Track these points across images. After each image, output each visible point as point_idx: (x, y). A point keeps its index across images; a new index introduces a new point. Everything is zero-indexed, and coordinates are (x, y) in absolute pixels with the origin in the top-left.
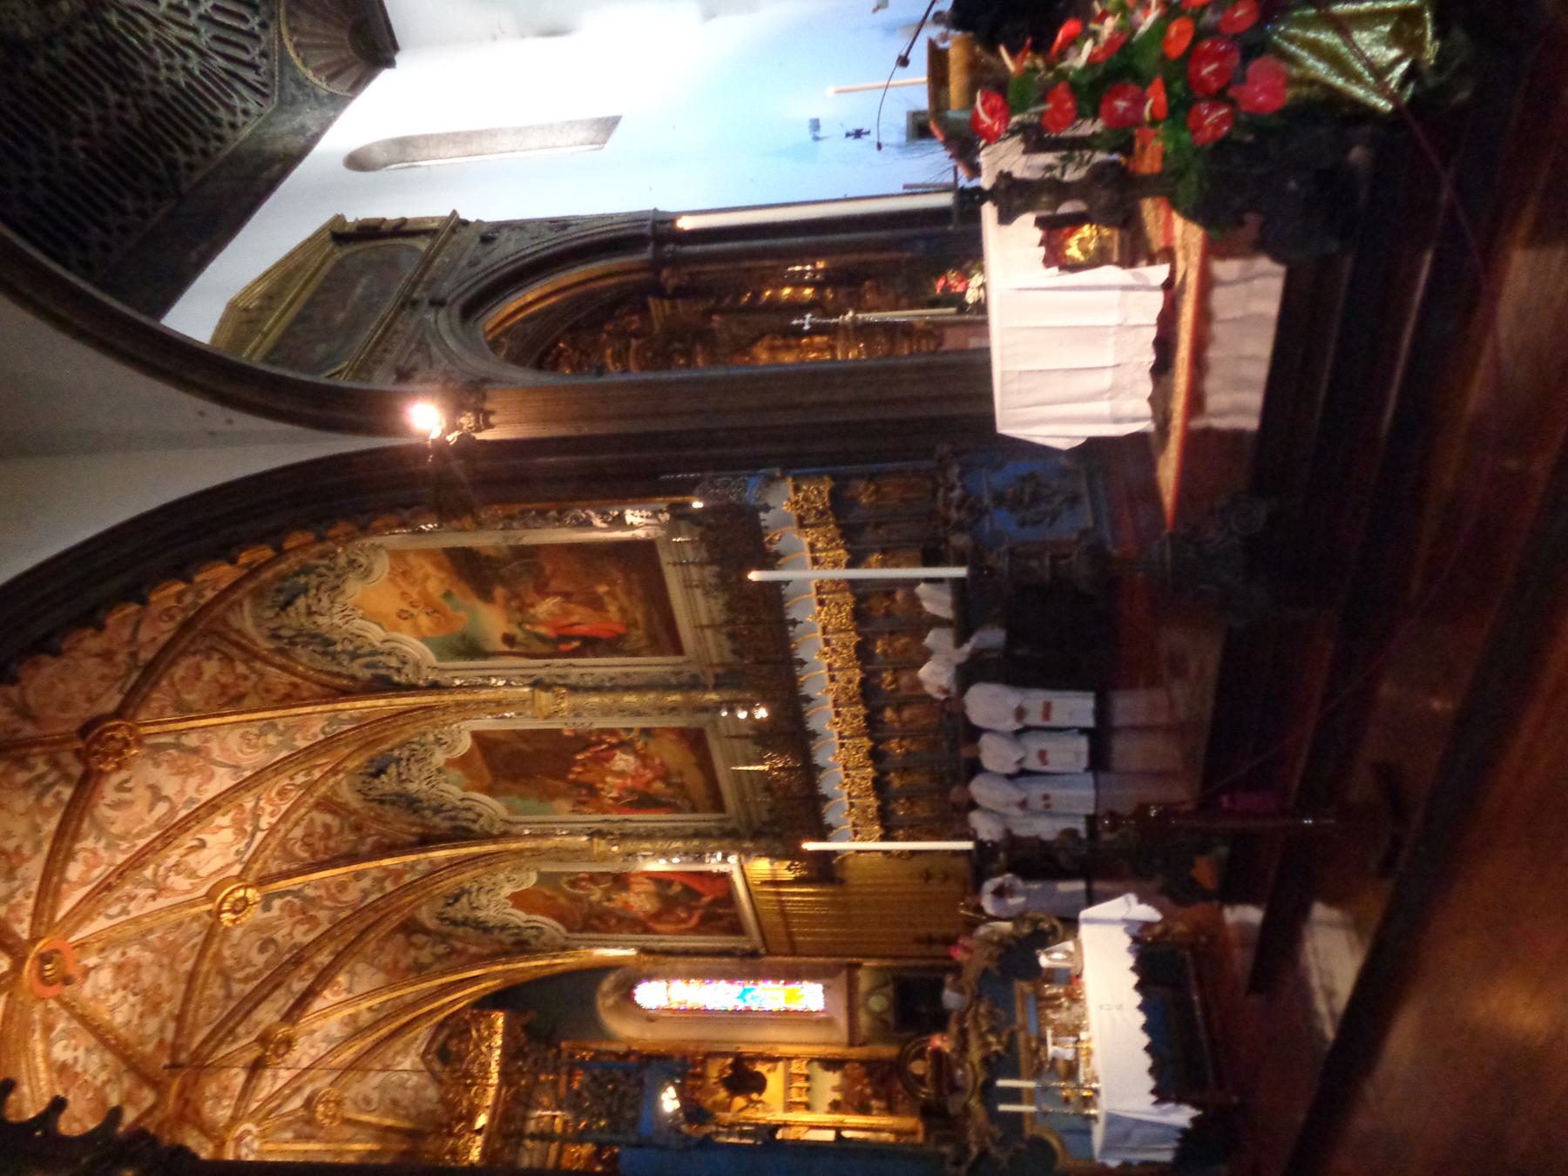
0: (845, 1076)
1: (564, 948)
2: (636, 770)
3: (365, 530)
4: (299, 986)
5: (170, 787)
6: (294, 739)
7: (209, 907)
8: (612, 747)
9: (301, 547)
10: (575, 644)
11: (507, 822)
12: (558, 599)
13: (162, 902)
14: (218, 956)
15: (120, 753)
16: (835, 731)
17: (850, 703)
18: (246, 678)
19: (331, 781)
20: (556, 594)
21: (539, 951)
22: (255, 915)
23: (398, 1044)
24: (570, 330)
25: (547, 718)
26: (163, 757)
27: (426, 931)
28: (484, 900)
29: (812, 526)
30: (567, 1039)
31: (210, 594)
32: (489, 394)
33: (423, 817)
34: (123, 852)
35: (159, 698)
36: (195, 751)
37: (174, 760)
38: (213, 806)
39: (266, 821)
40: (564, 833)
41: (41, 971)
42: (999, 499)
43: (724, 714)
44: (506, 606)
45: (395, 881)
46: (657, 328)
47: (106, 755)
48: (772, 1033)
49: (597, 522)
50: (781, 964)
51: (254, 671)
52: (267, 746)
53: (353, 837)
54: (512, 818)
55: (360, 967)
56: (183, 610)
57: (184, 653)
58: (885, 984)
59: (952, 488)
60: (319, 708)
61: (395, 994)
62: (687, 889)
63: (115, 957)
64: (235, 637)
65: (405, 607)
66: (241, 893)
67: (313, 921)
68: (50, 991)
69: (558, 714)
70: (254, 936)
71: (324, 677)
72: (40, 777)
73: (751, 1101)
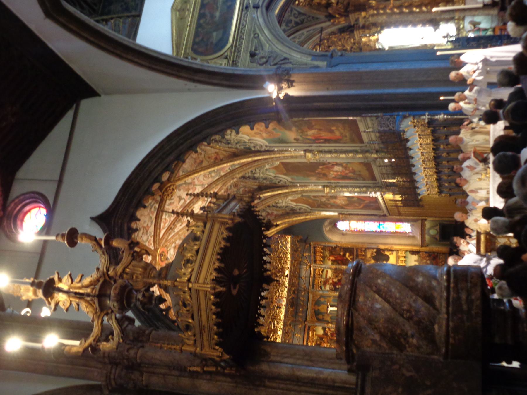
0: (420, 256)
6: (220, 173)
10: (321, 141)
11: (290, 182)
12: (316, 131)
16: (423, 168)
17: (429, 161)
18: (201, 154)
20: (315, 129)
21: (300, 213)
26: (181, 188)
30: (312, 241)
32: (292, 75)
36: (191, 183)
47: (168, 195)
48: (391, 241)
52: (211, 176)
53: (235, 190)
58: (437, 225)
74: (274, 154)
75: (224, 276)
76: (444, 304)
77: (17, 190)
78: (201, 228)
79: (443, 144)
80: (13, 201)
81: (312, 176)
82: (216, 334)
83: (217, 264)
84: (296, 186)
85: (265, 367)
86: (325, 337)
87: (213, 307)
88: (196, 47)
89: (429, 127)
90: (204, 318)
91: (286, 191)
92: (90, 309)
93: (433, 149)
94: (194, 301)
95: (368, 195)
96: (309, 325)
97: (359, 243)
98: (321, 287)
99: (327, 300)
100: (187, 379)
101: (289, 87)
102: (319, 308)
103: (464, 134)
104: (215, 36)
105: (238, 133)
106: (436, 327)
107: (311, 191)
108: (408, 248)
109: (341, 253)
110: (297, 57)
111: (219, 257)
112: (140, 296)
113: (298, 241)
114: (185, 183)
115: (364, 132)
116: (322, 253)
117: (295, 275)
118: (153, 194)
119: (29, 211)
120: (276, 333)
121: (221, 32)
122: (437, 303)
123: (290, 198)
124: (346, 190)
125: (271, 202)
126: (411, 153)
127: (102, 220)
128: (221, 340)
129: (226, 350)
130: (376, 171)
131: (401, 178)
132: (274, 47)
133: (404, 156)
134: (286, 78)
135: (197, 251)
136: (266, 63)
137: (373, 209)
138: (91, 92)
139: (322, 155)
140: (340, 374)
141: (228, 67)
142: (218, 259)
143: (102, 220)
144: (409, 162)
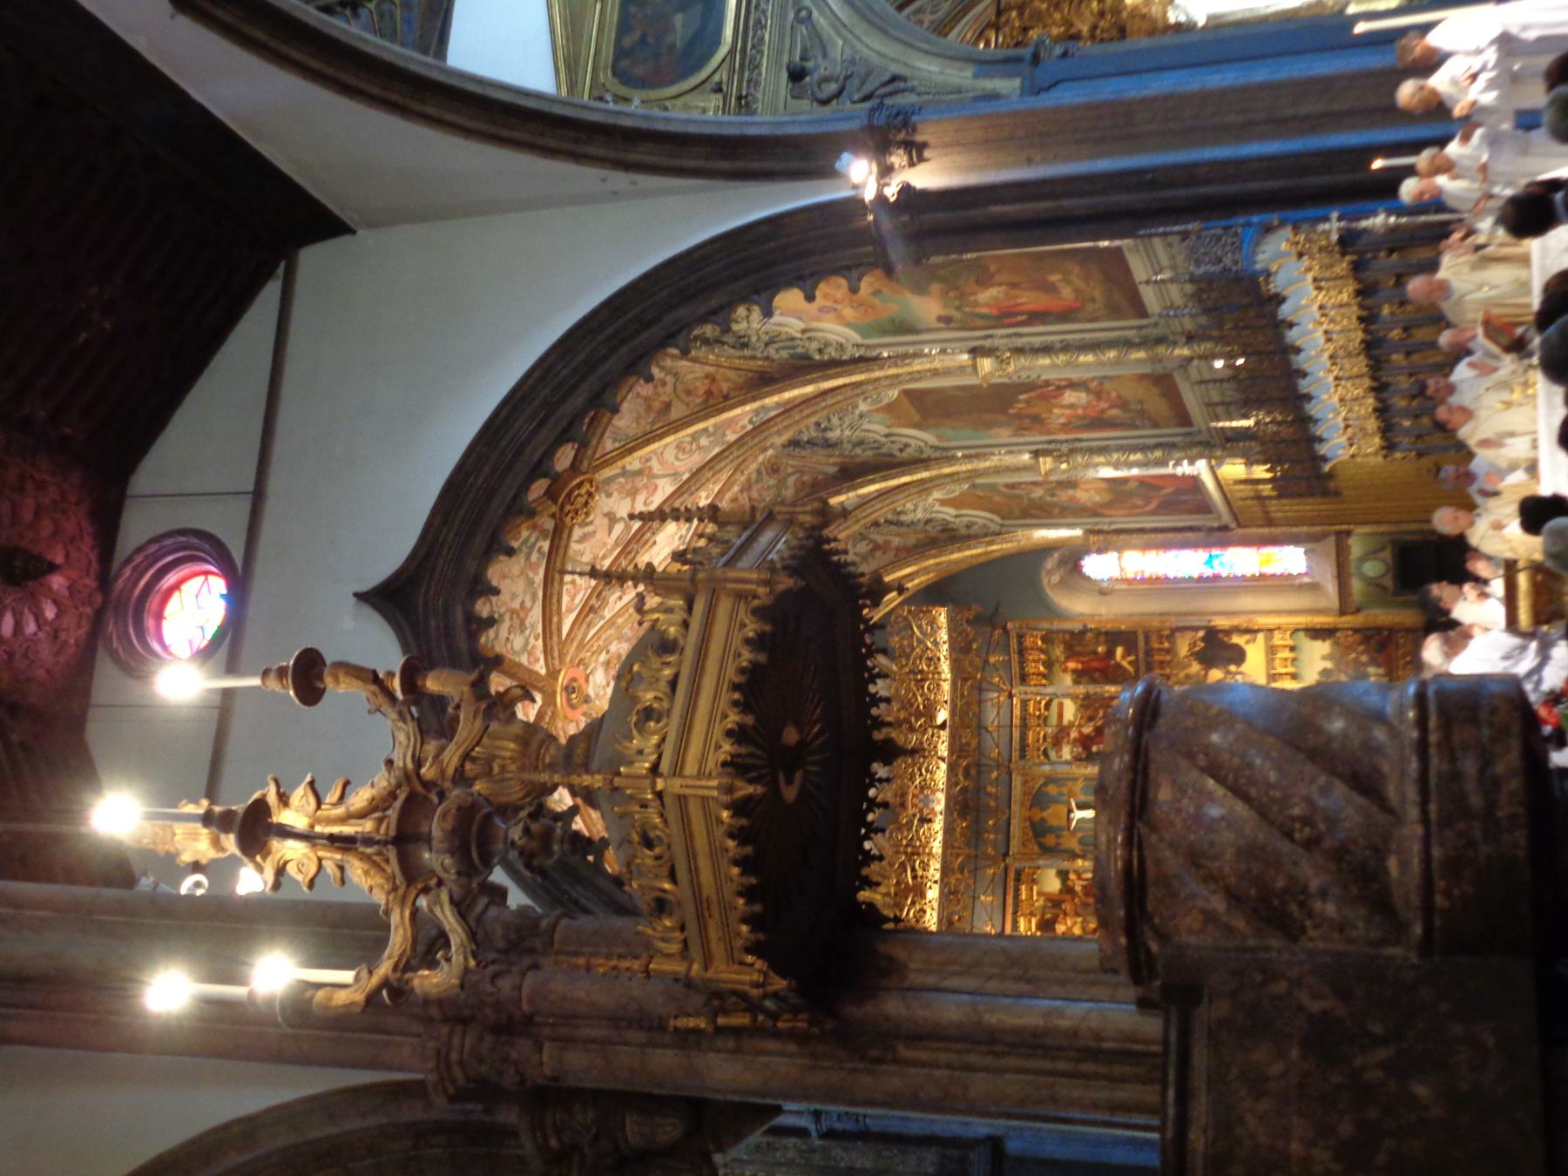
0: (1336, 644)
2: (1089, 403)
6: (724, 435)
10: (1020, 318)
11: (936, 448)
16: (1331, 378)
17: (1349, 355)
20: (1000, 284)
21: (969, 537)
26: (614, 487)
32: (919, 127)
36: (639, 473)
48: (1246, 602)
52: (699, 448)
53: (772, 482)
54: (942, 444)
58: (1383, 549)
72: (527, 540)
73: (1228, 672)
74: (881, 368)
75: (758, 750)
76: (1412, 793)
77: (137, 527)
78: (679, 616)
79: (1391, 303)
80: (128, 560)
81: (1001, 425)
82: (744, 921)
83: (733, 718)
84: (951, 460)
85: (893, 1006)
86: (1068, 897)
87: (731, 844)
88: (625, 63)
89: (1343, 254)
90: (706, 877)
91: (925, 475)
92: (378, 880)
93: (1361, 319)
94: (675, 827)
95: (1169, 470)
96: (1017, 865)
97: (1152, 614)
98: (1045, 753)
99: (1065, 790)
100: (670, 1052)
101: (912, 164)
102: (1045, 814)
103: (1453, 268)
104: (681, 25)
105: (768, 313)
106: (1392, 864)
107: (997, 471)
108: (1302, 620)
109: (1100, 649)
110: (930, 69)
111: (737, 696)
112: (516, 833)
113: (968, 622)
114: (624, 473)
115: (1148, 282)
116: (1042, 651)
117: (967, 720)
118: (532, 514)
119: (176, 587)
120: (923, 895)
121: (697, 10)
122: (1391, 792)
123: (937, 495)
124: (1101, 459)
125: (882, 512)
126: (1292, 335)
127: (392, 598)
128: (761, 936)
129: (778, 967)
130: (1191, 399)
131: (1269, 413)
132: (859, 46)
133: (1272, 347)
134: (902, 136)
135: (673, 684)
136: (838, 94)
137: (1190, 512)
138: (324, 224)
139: (1023, 361)
140: (1115, 1013)
141: (727, 118)
142: (735, 704)
143: (392, 598)
144: (1288, 363)
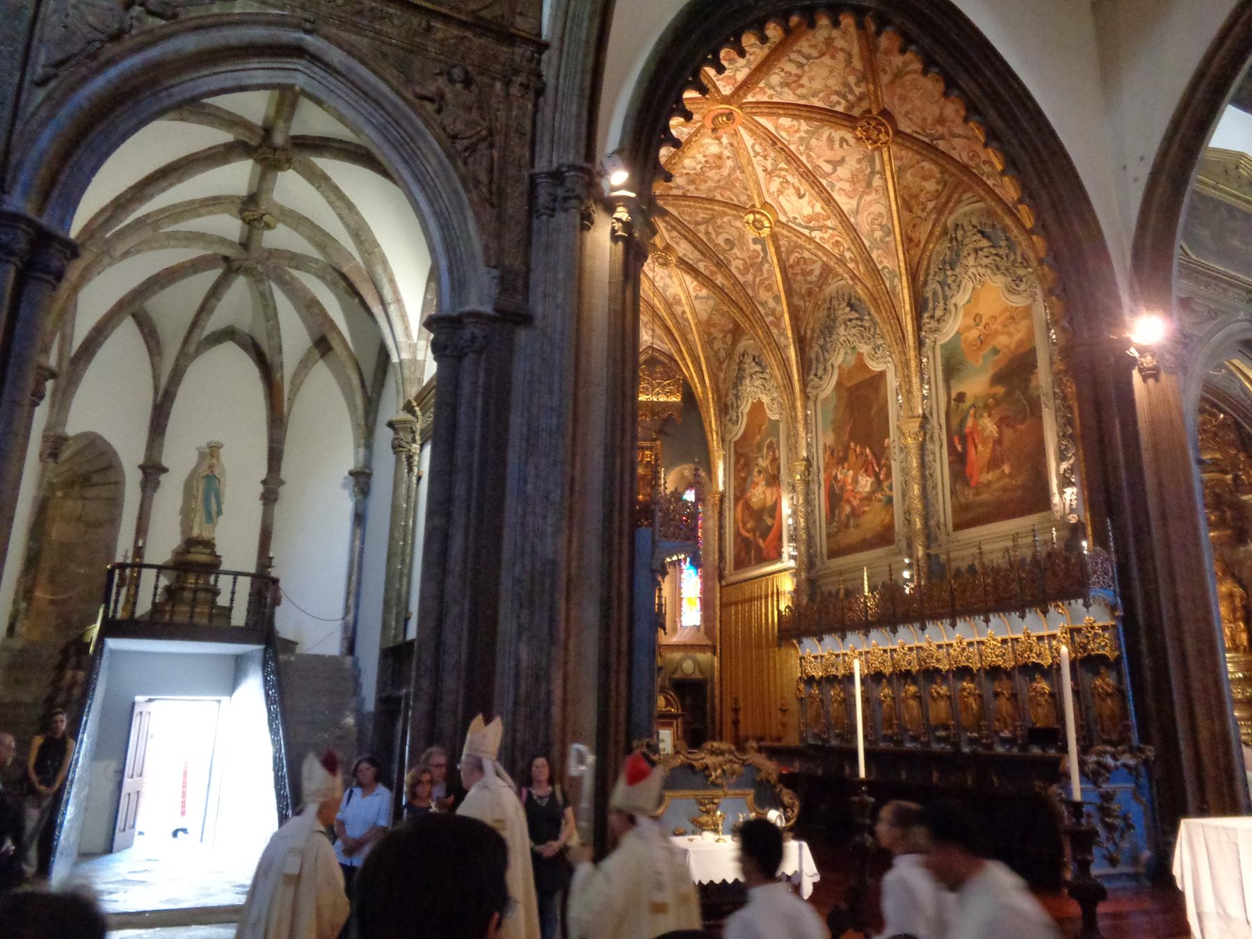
1: (723, 440)
3: (1049, 292)
4: (701, 266)
5: (843, 172)
6: (878, 249)
7: (758, 205)
8: (877, 476)
9: (1032, 245)
10: (959, 448)
13: (761, 175)
14: (724, 214)
15: (868, 139)
16: (897, 647)
19: (846, 276)
20: (1000, 433)
22: (751, 234)
23: (659, 331)
24: (1237, 424)
25: (899, 427)
26: (864, 164)
27: (735, 343)
28: (758, 383)
29: (1072, 638)
31: (990, 182)
33: (819, 337)
34: (798, 149)
35: (907, 155)
36: (869, 185)
37: (861, 171)
38: (829, 201)
39: (814, 234)
40: (809, 438)
41: (722, 115)
42: (1107, 797)
43: (907, 561)
44: (989, 396)
45: (772, 323)
46: (1245, 498)
49: (1064, 465)
50: (715, 596)
51: (928, 215)
52: (873, 231)
54: (819, 404)
55: (711, 302)
56: (978, 166)
57: (944, 171)
58: (702, 673)
59: (1115, 758)
60: (902, 264)
61: (693, 327)
62: (770, 528)
63: (727, 153)
64: (956, 196)
65: (984, 320)
66: (766, 224)
67: (746, 270)
68: (708, 123)
69: (901, 434)
70: (736, 235)
71: (925, 264)
72: (851, 91)
84: (805, 408)
104: (1204, 233)
109: (641, 497)
114: (873, 173)
133: (958, 608)
